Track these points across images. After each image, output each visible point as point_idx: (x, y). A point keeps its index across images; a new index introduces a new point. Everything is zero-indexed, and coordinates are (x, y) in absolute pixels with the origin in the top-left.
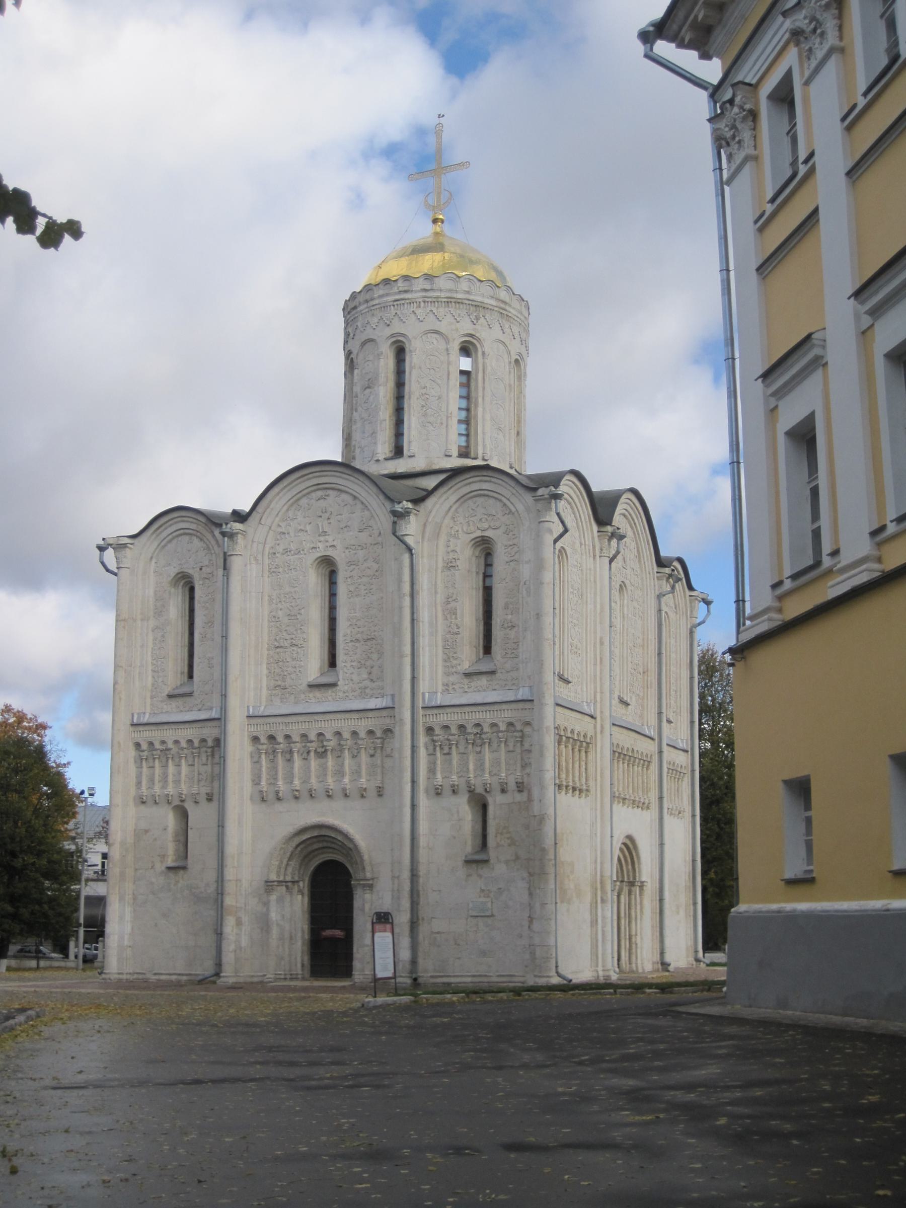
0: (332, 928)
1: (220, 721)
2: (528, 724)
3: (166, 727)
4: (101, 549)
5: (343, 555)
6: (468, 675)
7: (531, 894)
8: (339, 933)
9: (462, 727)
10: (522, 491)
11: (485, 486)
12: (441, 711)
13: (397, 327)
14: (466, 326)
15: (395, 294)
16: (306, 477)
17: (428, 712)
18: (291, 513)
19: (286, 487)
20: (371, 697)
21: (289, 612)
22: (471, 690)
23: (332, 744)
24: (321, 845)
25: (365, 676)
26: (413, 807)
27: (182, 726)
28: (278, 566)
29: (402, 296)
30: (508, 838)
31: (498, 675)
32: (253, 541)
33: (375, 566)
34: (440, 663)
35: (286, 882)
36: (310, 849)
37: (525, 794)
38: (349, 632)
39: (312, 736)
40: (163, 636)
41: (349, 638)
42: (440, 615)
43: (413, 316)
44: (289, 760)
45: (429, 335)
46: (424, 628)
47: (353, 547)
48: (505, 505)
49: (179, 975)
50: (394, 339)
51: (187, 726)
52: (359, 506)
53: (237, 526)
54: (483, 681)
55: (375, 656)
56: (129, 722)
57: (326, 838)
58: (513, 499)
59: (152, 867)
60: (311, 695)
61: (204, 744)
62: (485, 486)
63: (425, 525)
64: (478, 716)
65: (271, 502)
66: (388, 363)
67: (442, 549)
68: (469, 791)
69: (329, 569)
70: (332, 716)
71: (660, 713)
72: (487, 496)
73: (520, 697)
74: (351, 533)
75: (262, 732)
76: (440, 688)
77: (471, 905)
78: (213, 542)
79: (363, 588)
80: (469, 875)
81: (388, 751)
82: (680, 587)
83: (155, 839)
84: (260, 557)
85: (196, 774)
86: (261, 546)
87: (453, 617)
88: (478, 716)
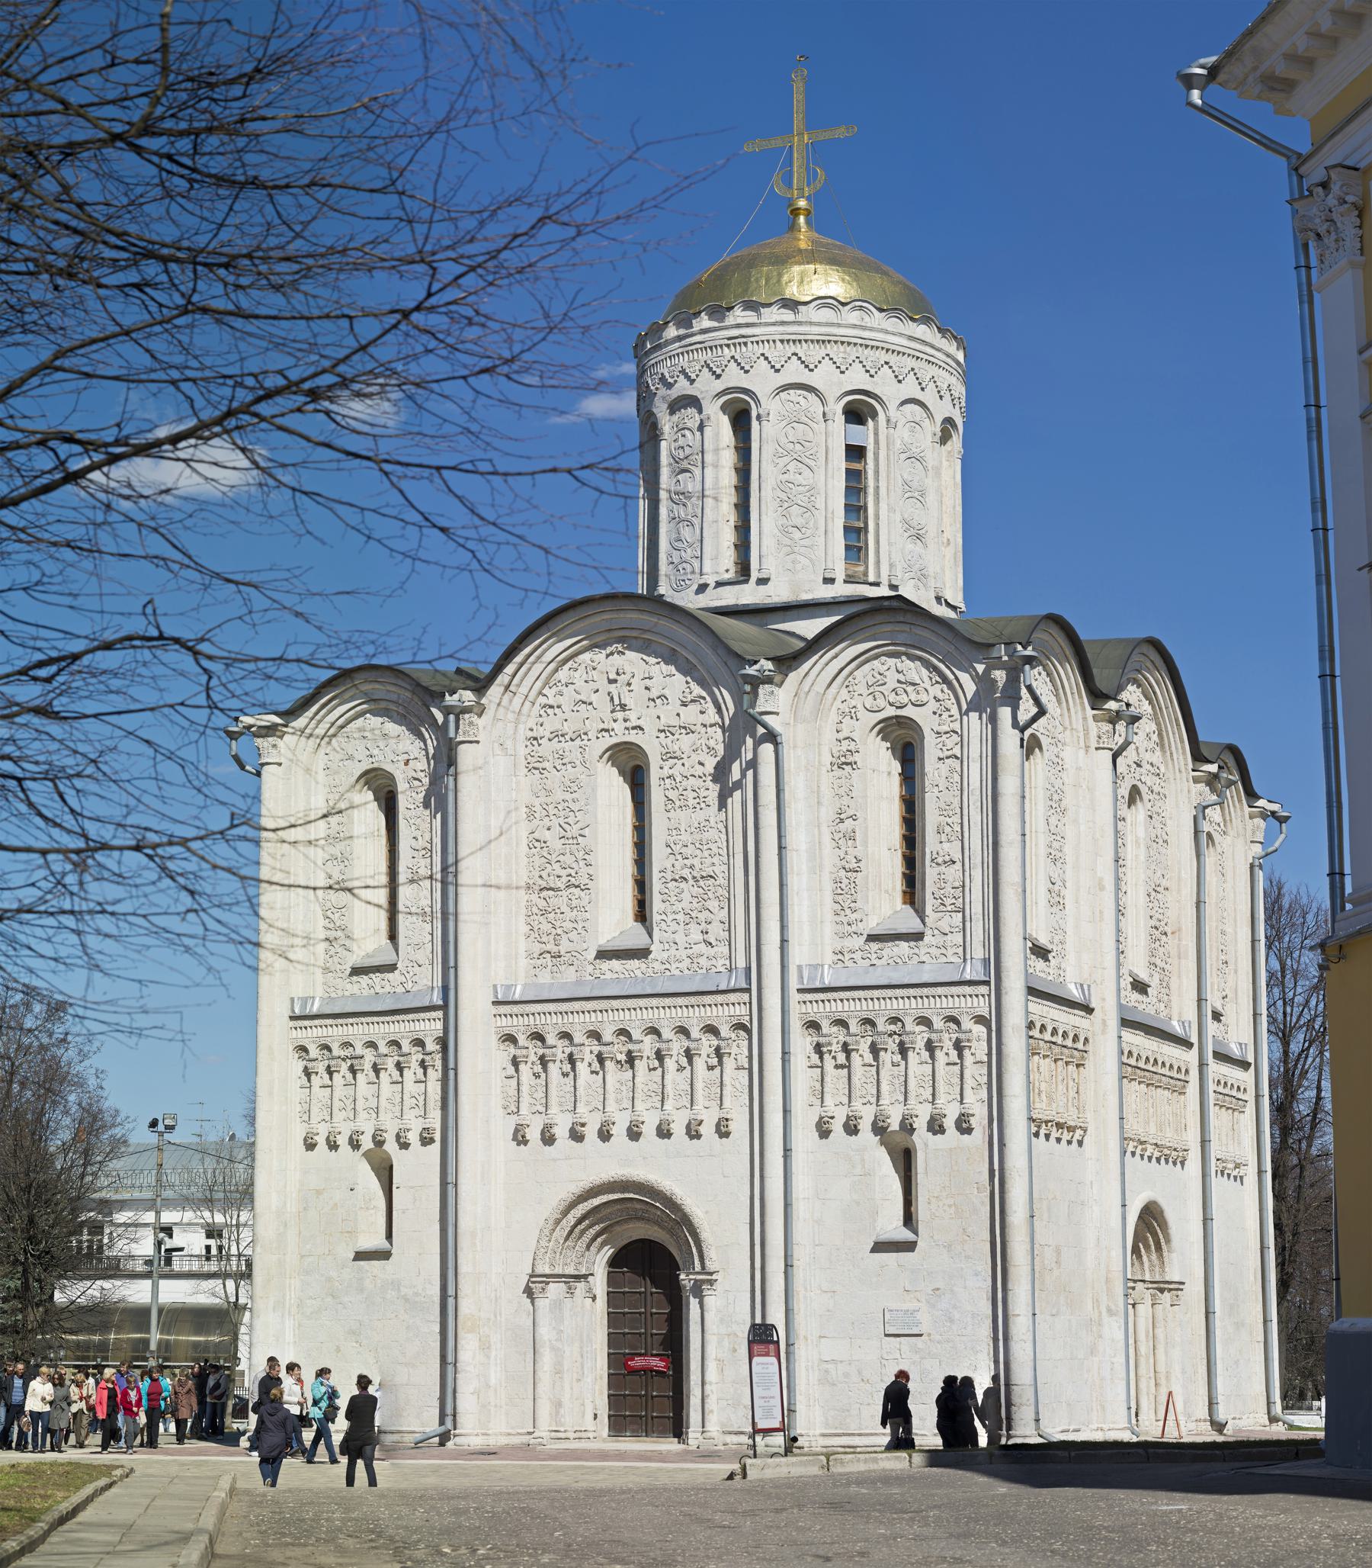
6: (872, 938)
22: (883, 961)
25: (700, 937)
34: (829, 916)
45: (792, 392)
46: (797, 861)
53: (468, 697)
55: (713, 905)
66: (722, 429)
71: (1200, 1000)
75: (520, 1027)
76: (829, 958)
82: (1235, 794)
87: (850, 842)
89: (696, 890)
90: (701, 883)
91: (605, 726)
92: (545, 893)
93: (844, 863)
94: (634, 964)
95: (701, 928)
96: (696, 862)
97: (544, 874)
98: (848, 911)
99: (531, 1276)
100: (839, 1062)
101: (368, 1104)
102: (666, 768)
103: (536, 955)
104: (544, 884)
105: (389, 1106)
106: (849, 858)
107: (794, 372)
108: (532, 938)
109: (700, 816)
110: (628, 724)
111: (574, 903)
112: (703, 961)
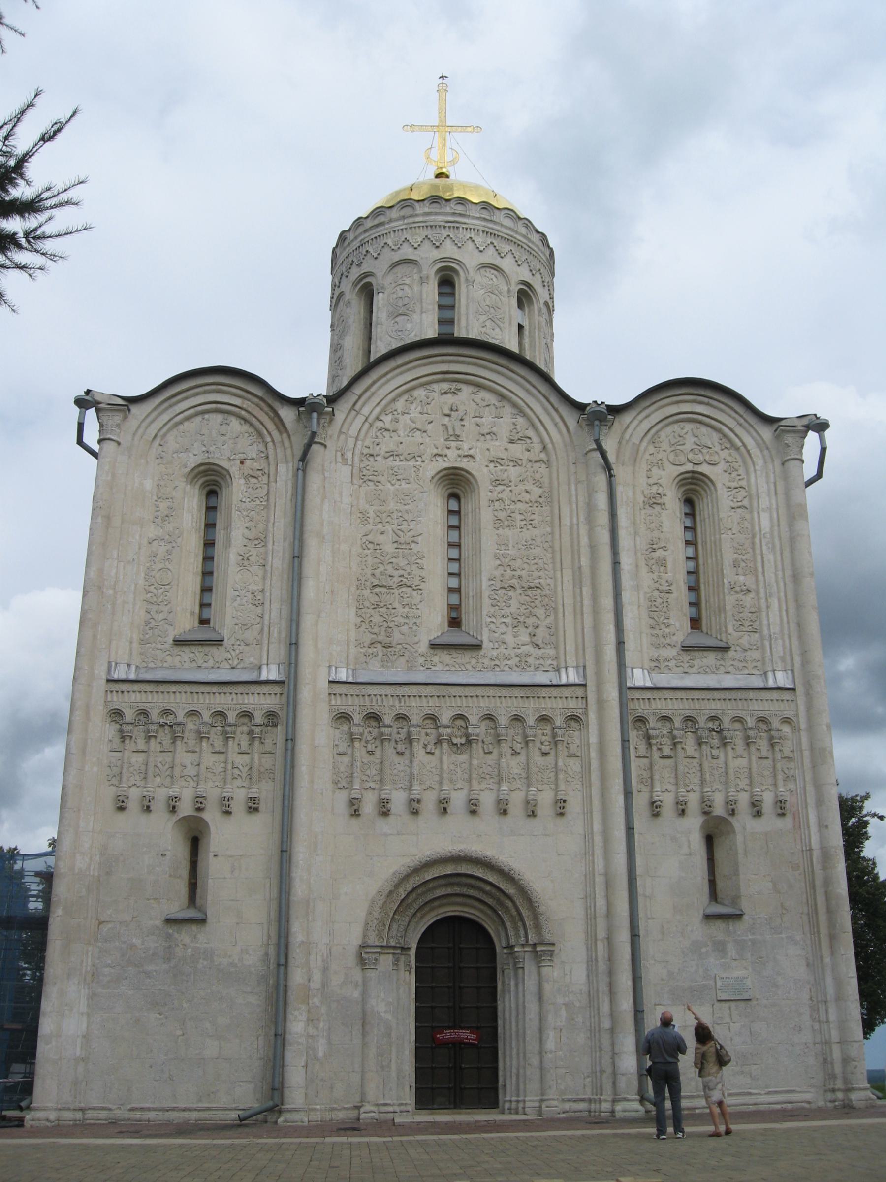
0: (454, 1027)
1: (288, 685)
2: (786, 721)
3: (174, 688)
4: (83, 403)
5: (485, 470)
6: (686, 649)
8: (466, 1035)
9: (689, 719)
10: (752, 420)
12: (656, 694)
13: (449, 250)
14: (526, 276)
17: (637, 695)
18: (400, 405)
20: (537, 669)
21: (396, 538)
22: (694, 670)
23: (479, 730)
24: (449, 891)
25: (525, 638)
26: (630, 830)
27: (207, 689)
28: (376, 473)
31: (731, 653)
33: (536, 491)
35: (394, 947)
36: (430, 896)
37: (788, 819)
38: (497, 573)
39: (445, 717)
40: (169, 552)
41: (498, 585)
42: (642, 563)
43: (470, 241)
44: (400, 754)
45: (488, 270)
48: (725, 436)
49: (184, 1110)
51: (215, 689)
52: (508, 410)
54: (711, 658)
55: (540, 612)
56: (104, 677)
57: (465, 880)
58: (738, 430)
60: (436, 659)
61: (246, 720)
64: (713, 706)
65: (374, 383)
66: (431, 291)
67: (642, 480)
68: (706, 813)
69: (456, 485)
70: (479, 691)
73: (771, 684)
74: (497, 443)
75: (355, 707)
78: (271, 426)
79: (519, 517)
81: (573, 748)
84: (349, 455)
85: (230, 766)
86: (351, 442)
87: (662, 569)
88: (713, 706)
89: (523, 599)
90: (529, 593)
91: (439, 451)
92: (377, 590)
93: (657, 585)
94: (465, 658)
95: (528, 631)
96: (524, 573)
97: (377, 572)
98: (663, 626)
99: (362, 947)
100: (665, 754)
101: (185, 772)
102: (495, 493)
103: (365, 644)
104: (376, 582)
105: (210, 775)
106: (663, 582)
107: (490, 256)
108: (362, 629)
109: (527, 534)
110: (460, 452)
111: (406, 601)
112: (531, 660)
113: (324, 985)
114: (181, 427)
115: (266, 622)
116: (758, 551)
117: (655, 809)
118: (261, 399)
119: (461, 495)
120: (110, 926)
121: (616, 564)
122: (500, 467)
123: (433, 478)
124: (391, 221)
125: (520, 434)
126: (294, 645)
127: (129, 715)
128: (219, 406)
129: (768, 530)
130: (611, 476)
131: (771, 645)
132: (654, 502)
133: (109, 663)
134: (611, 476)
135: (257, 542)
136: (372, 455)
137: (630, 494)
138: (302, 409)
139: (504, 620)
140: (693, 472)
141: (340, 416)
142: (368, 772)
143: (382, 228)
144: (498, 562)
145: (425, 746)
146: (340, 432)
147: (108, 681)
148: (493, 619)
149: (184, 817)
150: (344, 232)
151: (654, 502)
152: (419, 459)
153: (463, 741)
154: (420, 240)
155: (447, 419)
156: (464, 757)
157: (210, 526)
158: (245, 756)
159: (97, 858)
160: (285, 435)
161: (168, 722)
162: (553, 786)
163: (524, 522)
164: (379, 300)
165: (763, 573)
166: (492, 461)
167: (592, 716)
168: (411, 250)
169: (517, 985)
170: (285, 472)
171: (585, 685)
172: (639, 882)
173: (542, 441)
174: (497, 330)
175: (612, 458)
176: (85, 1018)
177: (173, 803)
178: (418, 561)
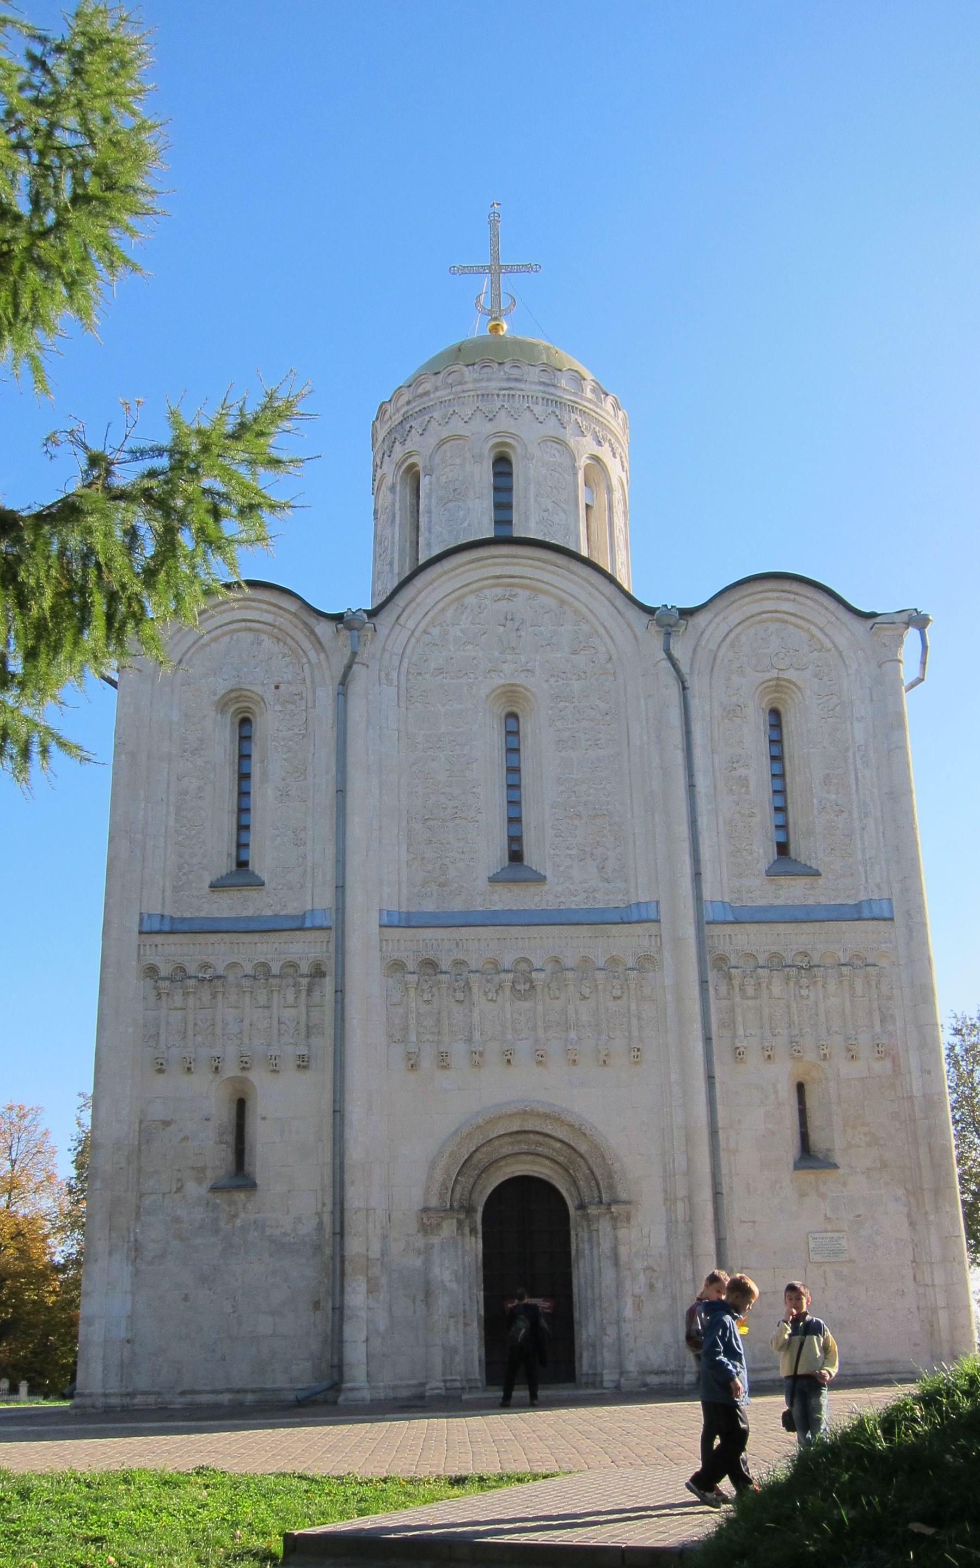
5: (545, 686)
7: (912, 1224)
11: (786, 606)
13: (504, 423)
15: (502, 380)
16: (481, 563)
19: (445, 573)
24: (516, 1149)
26: (710, 1078)
29: (512, 385)
30: (865, 1135)
32: (384, 649)
45: (549, 444)
47: (563, 676)
48: (813, 636)
50: (499, 440)
56: (136, 930)
59: (179, 1190)
60: (496, 897)
61: (291, 970)
62: (786, 606)
63: (695, 650)
65: (420, 592)
72: (786, 622)
77: (812, 1245)
78: (307, 645)
80: (802, 1195)
83: (186, 1138)
85: (275, 1022)
92: (429, 823)
113: (384, 1253)
114: (208, 649)
115: (309, 864)
116: (851, 767)
117: (738, 1054)
118: (295, 615)
119: (520, 714)
120: (153, 1197)
121: (691, 786)
122: (561, 682)
123: (488, 696)
124: (437, 389)
125: (583, 644)
126: (340, 888)
127: (165, 970)
128: (248, 624)
129: (862, 742)
130: (684, 688)
131: (866, 872)
132: (733, 712)
133: (141, 914)
134: (684, 688)
135: (296, 775)
136: (420, 674)
137: (707, 708)
138: (341, 626)
139: (569, 852)
140: (778, 679)
141: (383, 631)
142: (425, 1023)
143: (425, 398)
144: (562, 788)
145: (486, 994)
146: (384, 649)
147: (141, 933)
148: (557, 852)
149: (229, 1079)
150: (384, 403)
151: (733, 712)
152: (472, 675)
153: (527, 986)
154: (470, 412)
155: (502, 628)
156: (526, 1005)
157: (244, 757)
158: (292, 1010)
159: (137, 1126)
160: (322, 656)
161: (207, 976)
162: (626, 1034)
163: (589, 743)
164: (424, 482)
165: (857, 791)
166: (552, 676)
167: (667, 955)
168: (461, 424)
169: (591, 1249)
170: (325, 696)
171: (658, 921)
172: (721, 1135)
173: (608, 651)
174: (562, 515)
175: (685, 669)
176: (129, 1297)
177: (216, 1064)
178: (474, 790)
